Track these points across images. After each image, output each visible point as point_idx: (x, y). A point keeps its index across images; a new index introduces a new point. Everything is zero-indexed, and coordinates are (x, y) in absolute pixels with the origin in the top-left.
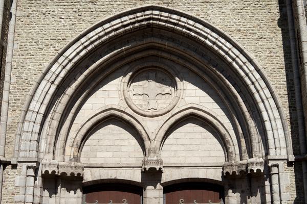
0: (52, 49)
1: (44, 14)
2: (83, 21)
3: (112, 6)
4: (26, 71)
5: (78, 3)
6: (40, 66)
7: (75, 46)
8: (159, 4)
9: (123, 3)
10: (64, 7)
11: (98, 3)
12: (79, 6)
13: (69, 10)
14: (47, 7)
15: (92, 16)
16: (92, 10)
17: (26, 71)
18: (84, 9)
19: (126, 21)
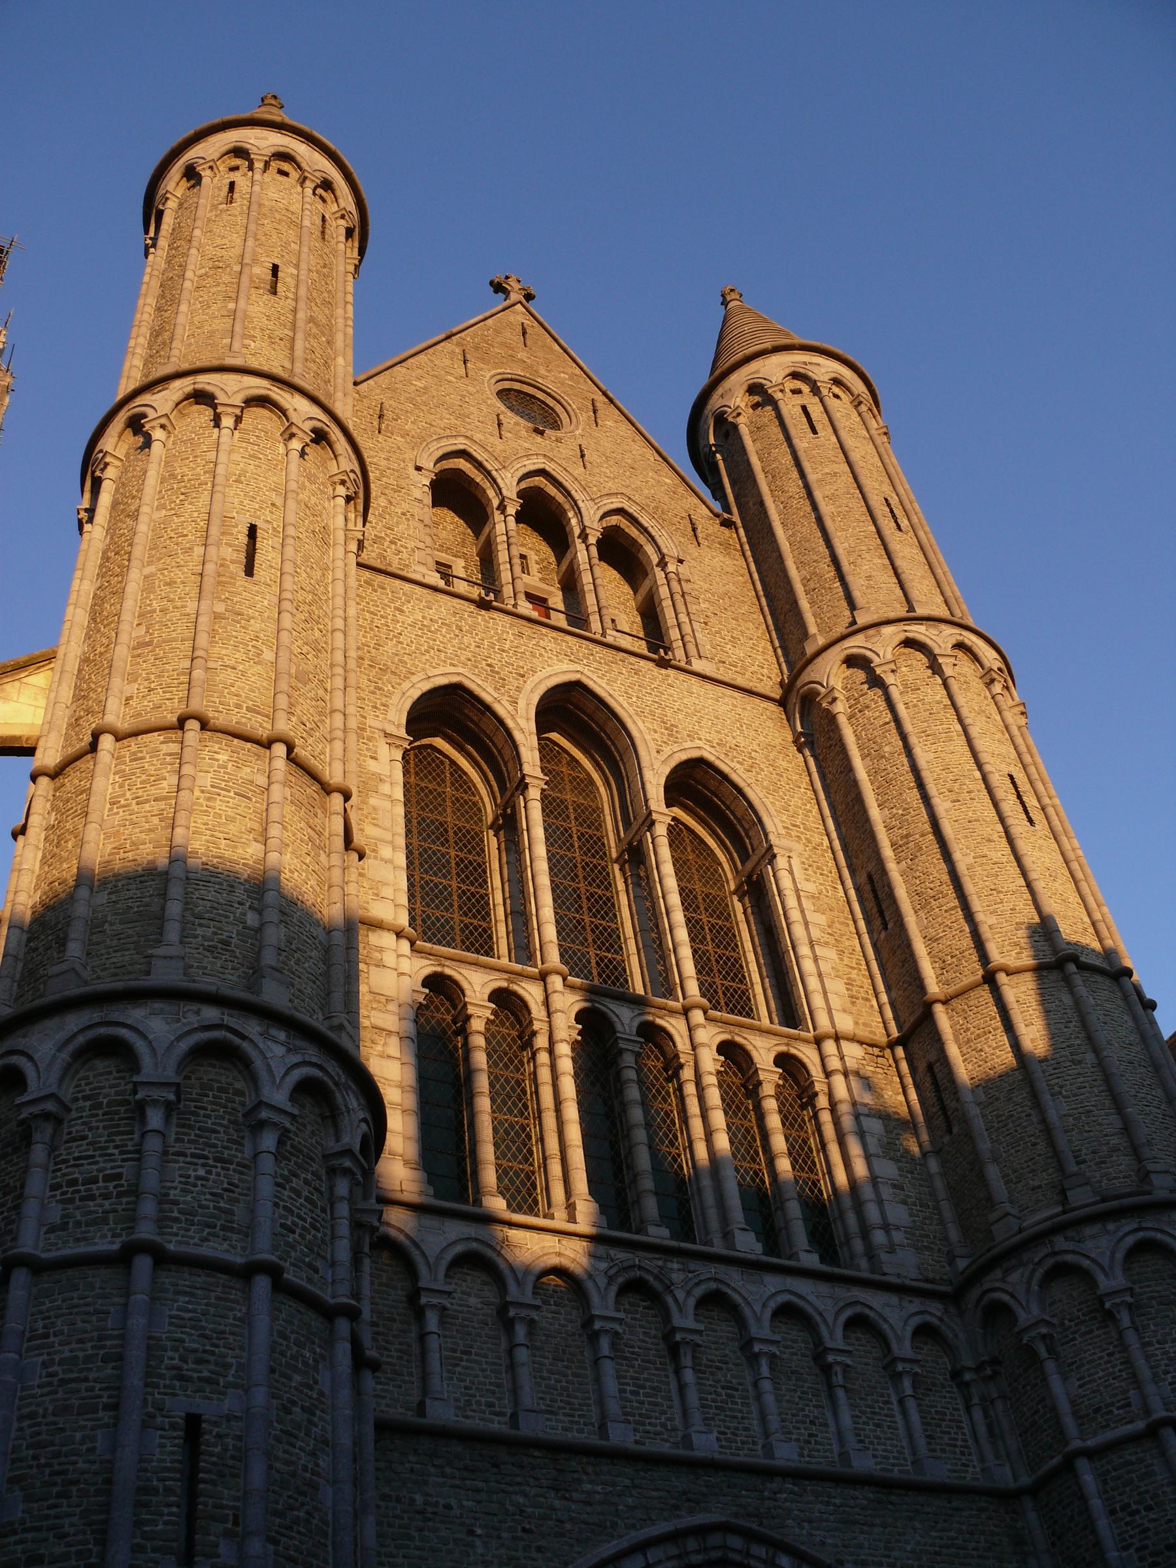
1: (418, 1512)
2: (539, 1549)
5: (516, 1488)
8: (736, 1515)
11: (575, 1495)
12: (521, 1500)
15: (562, 1535)
18: (537, 1511)
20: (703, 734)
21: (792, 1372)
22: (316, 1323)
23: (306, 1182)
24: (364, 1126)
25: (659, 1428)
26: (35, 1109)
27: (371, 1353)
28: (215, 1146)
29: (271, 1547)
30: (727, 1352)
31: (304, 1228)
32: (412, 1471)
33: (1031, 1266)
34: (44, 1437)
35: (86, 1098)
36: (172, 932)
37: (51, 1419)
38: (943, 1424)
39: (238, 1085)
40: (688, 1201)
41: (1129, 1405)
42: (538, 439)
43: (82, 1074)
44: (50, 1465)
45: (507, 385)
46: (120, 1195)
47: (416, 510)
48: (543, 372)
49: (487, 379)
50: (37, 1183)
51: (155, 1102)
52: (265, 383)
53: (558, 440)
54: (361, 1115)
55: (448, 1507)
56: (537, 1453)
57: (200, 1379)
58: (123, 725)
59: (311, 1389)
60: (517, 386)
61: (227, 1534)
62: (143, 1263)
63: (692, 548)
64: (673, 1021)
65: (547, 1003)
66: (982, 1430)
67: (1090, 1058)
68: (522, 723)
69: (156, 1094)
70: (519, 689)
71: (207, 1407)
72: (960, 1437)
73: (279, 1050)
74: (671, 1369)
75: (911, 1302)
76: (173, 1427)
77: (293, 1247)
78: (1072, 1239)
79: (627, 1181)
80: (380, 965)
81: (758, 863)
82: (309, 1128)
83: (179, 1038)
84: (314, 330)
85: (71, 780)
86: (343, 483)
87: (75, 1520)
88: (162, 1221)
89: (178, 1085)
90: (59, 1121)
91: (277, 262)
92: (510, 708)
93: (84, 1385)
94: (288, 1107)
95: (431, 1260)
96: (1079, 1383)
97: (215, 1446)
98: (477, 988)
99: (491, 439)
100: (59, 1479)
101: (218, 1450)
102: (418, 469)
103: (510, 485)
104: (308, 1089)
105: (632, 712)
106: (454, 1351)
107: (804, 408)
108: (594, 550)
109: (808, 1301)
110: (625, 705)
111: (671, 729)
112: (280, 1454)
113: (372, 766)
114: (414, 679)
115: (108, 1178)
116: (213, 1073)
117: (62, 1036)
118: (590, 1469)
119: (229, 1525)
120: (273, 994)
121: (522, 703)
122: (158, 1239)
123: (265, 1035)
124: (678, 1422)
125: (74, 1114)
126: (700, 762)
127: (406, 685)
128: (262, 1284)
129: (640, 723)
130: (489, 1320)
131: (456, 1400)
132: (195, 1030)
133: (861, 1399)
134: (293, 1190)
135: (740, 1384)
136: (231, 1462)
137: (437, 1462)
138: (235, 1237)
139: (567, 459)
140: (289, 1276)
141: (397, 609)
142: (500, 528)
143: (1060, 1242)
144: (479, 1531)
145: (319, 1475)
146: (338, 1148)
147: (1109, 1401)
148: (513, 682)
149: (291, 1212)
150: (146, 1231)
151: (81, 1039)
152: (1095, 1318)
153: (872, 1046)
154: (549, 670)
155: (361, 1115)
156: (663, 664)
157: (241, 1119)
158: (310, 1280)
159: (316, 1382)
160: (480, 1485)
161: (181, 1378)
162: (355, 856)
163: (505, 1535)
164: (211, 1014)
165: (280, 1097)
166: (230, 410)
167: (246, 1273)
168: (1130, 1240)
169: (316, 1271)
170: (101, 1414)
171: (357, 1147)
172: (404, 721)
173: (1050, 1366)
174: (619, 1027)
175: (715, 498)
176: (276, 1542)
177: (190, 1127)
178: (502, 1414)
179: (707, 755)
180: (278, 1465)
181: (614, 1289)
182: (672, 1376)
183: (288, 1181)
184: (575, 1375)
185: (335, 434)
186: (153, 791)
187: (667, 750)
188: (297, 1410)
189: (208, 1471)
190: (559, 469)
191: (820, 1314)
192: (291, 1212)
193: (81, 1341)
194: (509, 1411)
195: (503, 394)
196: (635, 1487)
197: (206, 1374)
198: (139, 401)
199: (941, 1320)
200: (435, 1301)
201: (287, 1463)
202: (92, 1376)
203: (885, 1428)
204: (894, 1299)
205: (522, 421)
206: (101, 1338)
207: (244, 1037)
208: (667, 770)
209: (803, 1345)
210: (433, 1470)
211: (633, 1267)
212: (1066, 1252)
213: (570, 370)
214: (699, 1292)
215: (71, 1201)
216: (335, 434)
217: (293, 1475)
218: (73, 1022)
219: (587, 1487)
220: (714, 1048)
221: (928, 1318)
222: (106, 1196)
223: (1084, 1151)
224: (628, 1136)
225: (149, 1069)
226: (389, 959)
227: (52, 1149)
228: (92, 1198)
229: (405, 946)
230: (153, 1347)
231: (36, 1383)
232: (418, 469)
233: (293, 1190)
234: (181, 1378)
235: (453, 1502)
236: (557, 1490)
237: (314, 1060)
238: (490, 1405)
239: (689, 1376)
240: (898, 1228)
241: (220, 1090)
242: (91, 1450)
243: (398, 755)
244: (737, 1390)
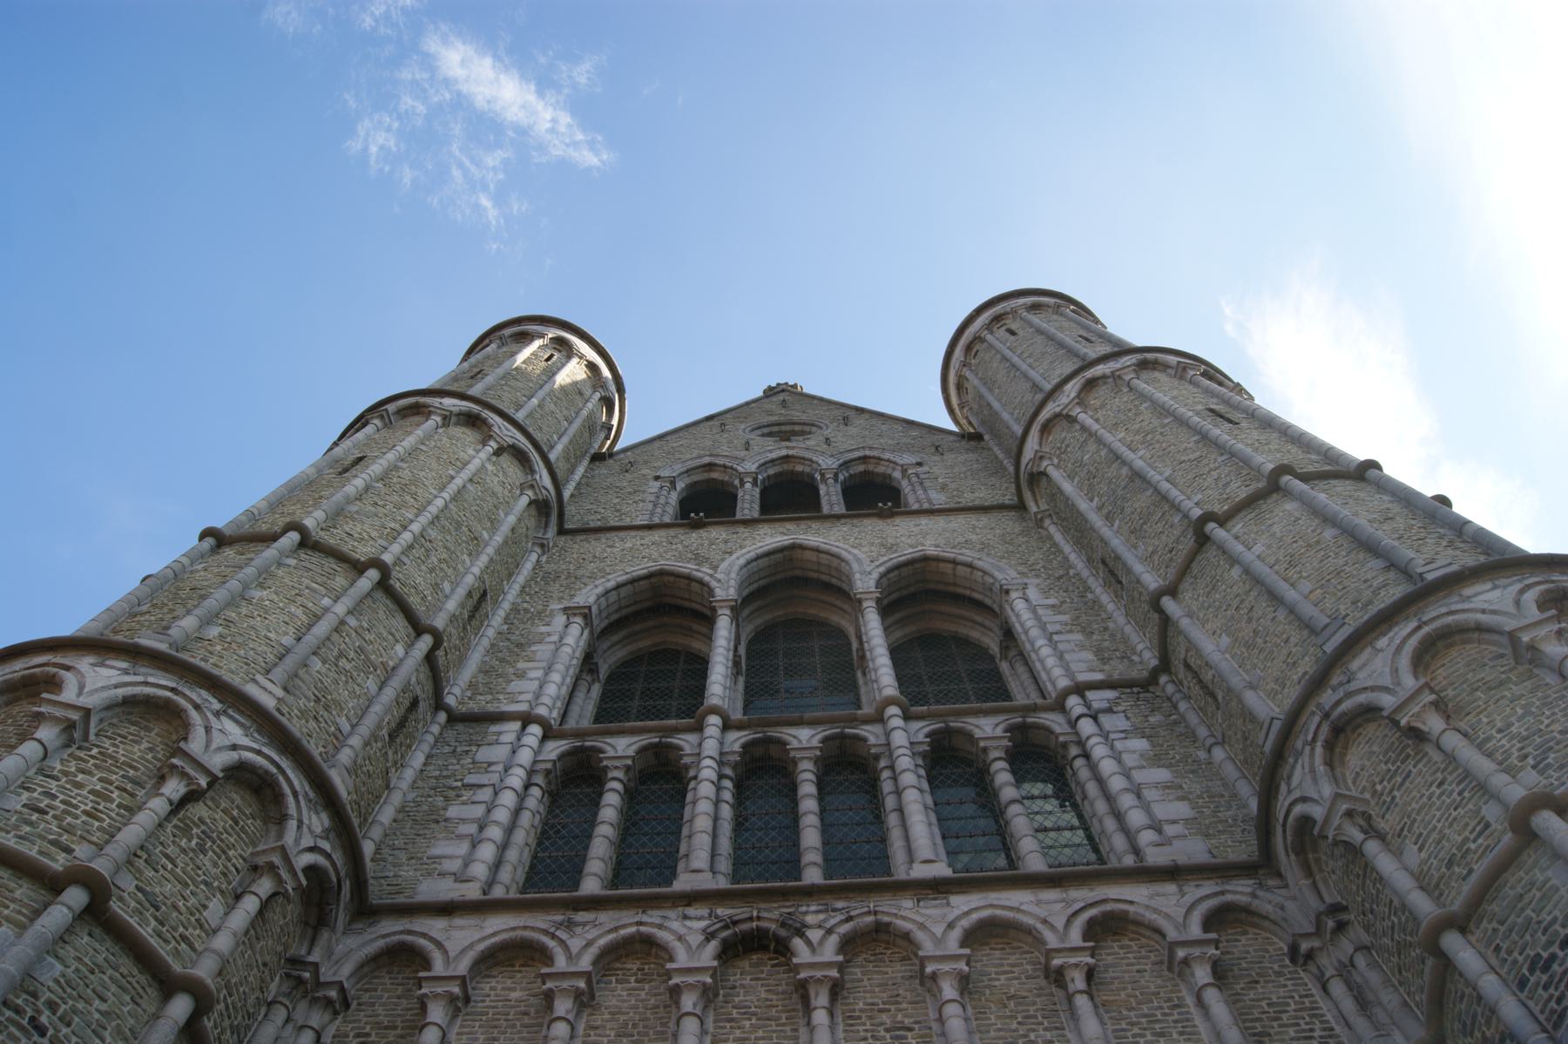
21: (1010, 998)
30: (901, 992)
33: (1308, 748)
38: (1284, 1016)
41: (1487, 826)
60: (776, 429)
66: (1348, 1005)
67: (1329, 533)
72: (1318, 1026)
75: (1197, 886)
78: (1341, 684)
92: (710, 572)
96: (1417, 846)
109: (1024, 912)
130: (532, 1010)
133: (1129, 1010)
135: (917, 1022)
141: (609, 546)
143: (1327, 698)
147: (1460, 839)
152: (1408, 756)
153: (1131, 687)
168: (1413, 642)
173: (1372, 847)
191: (1045, 922)
199: (1254, 895)
203: (1175, 1036)
204: (1171, 888)
209: (1029, 967)
212: (1338, 703)
221: (1229, 897)
223: (1342, 607)
240: (1174, 822)
244: (910, 1029)
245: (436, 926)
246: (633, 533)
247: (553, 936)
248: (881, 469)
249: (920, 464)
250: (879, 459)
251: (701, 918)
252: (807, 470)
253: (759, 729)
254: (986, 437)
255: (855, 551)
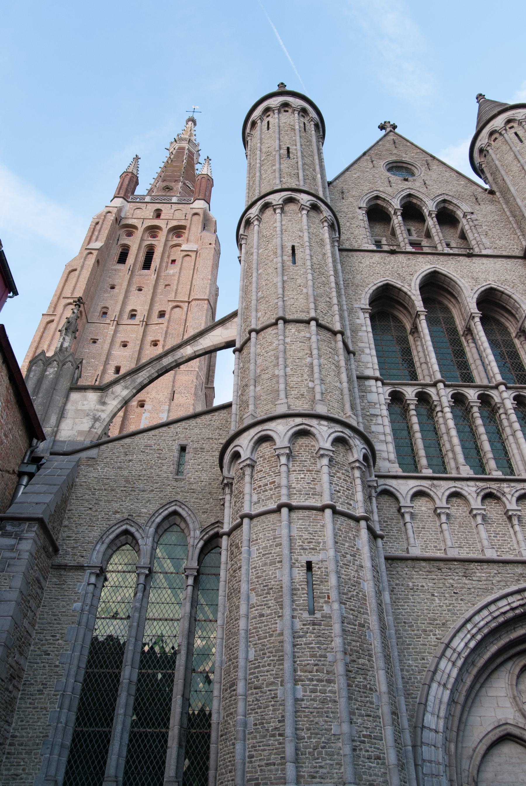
0: (432, 636)
2: (462, 600)
3: (491, 582)
4: (407, 668)
5: (449, 577)
6: (423, 661)
7: (461, 635)
9: (504, 579)
10: (434, 581)
11: (474, 578)
12: (452, 581)
13: (441, 585)
14: (413, 580)
15: (471, 594)
16: (469, 586)
17: (407, 668)
18: (459, 585)
19: (514, 602)
20: (491, 278)
22: (352, 523)
23: (343, 474)
24: (364, 451)
25: (507, 550)
26: (244, 464)
27: (379, 532)
28: (306, 466)
29: (343, 606)
31: (344, 490)
32: (406, 574)
34: (260, 574)
35: (261, 457)
36: (282, 395)
37: (261, 568)
39: (312, 444)
40: (509, 460)
42: (406, 183)
43: (259, 449)
44: (262, 584)
45: (391, 165)
46: (275, 488)
47: (362, 224)
48: (404, 156)
49: (381, 164)
50: (247, 489)
51: (282, 454)
52: (290, 193)
53: (414, 180)
54: (362, 446)
55: (423, 586)
56: (456, 563)
57: (310, 549)
58: (259, 327)
59: (353, 548)
60: (395, 165)
61: (326, 602)
62: (285, 511)
63: (477, 207)
64: (492, 391)
65: (438, 394)
68: (414, 292)
69: (282, 451)
70: (411, 280)
71: (311, 558)
73: (325, 428)
74: (510, 526)
76: (302, 566)
77: (340, 498)
79: (482, 455)
80: (371, 392)
81: (522, 323)
82: (342, 454)
83: (288, 431)
84: (307, 167)
85: (245, 351)
86: (326, 221)
87: (272, 601)
88: (289, 495)
89: (289, 447)
90: (253, 467)
91: (288, 146)
92: (408, 288)
93: (270, 555)
94: (331, 448)
95: (404, 496)
97: (318, 571)
98: (410, 393)
99: (387, 188)
100: (266, 588)
101: (319, 573)
102: (360, 208)
103: (396, 204)
104: (340, 441)
105: (458, 276)
106: (418, 528)
107: (516, 134)
108: (435, 219)
110: (455, 275)
111: (476, 280)
112: (343, 572)
113: (358, 321)
114: (370, 286)
115: (271, 483)
116: (303, 441)
117: (250, 437)
118: (479, 568)
119: (326, 599)
120: (321, 409)
121: (413, 285)
122: (289, 502)
123: (319, 424)
124: (516, 546)
125: (258, 463)
126: (491, 289)
127: (367, 289)
128: (328, 512)
129: (463, 281)
131: (422, 546)
132: (293, 427)
134: (338, 477)
136: (324, 577)
137: (417, 570)
138: (317, 497)
139: (419, 187)
140: (339, 508)
142: (396, 221)
144: (436, 595)
145: (360, 579)
146: (353, 460)
148: (408, 278)
149: (338, 485)
150: (284, 500)
151: (256, 437)
154: (423, 270)
155: (362, 446)
156: (470, 256)
157: (315, 455)
158: (348, 509)
159: (355, 545)
160: (434, 577)
161: (304, 549)
162: (352, 355)
163: (447, 595)
164: (298, 420)
165: (328, 445)
166: (278, 206)
167: (322, 509)
169: (351, 505)
170: (277, 564)
171: (361, 459)
172: (368, 302)
174: (469, 397)
175: (486, 184)
176: (345, 604)
177: (297, 461)
178: (441, 550)
179: (493, 286)
180: (343, 576)
181: (480, 498)
182: (511, 529)
183: (335, 474)
184: (469, 532)
185: (320, 204)
186: (270, 348)
187: (476, 289)
188: (348, 556)
189: (317, 581)
190: (416, 192)
192: (338, 485)
193: (268, 540)
194: (443, 548)
195: (389, 170)
196: (499, 573)
197: (312, 546)
198: (248, 213)
200: (407, 510)
201: (346, 575)
202: (273, 552)
205: (398, 178)
206: (274, 539)
207: (311, 426)
208: (476, 296)
210: (414, 573)
211: (487, 488)
213: (415, 151)
214: (517, 494)
215: (260, 493)
216: (320, 204)
217: (349, 579)
218: (253, 432)
219: (478, 574)
220: (512, 399)
222: (271, 490)
224: (479, 439)
225: (279, 444)
226: (374, 389)
227: (252, 477)
228: (266, 491)
229: (379, 383)
230: (291, 539)
231: (255, 556)
232: (360, 208)
233: (338, 477)
234: (304, 549)
235: (424, 584)
236: (466, 577)
237: (339, 430)
238: (435, 547)
239: (517, 528)
241: (306, 446)
242: (275, 577)
243: (367, 315)
245: (394, 483)
246: (366, 254)
247: (431, 490)
248: (451, 207)
249: (472, 213)
250: (451, 202)
251: (472, 487)
252: (419, 203)
253: (455, 388)
254: (497, 194)
255: (463, 281)
